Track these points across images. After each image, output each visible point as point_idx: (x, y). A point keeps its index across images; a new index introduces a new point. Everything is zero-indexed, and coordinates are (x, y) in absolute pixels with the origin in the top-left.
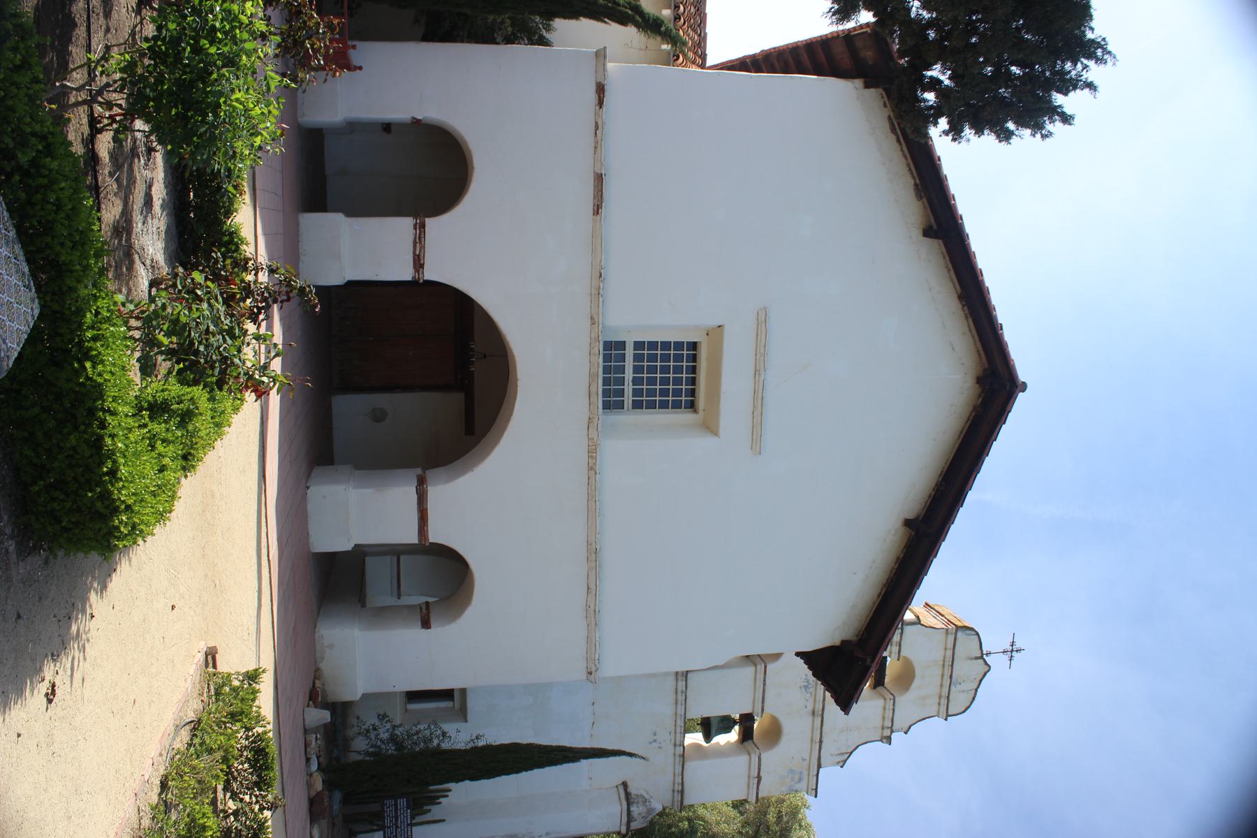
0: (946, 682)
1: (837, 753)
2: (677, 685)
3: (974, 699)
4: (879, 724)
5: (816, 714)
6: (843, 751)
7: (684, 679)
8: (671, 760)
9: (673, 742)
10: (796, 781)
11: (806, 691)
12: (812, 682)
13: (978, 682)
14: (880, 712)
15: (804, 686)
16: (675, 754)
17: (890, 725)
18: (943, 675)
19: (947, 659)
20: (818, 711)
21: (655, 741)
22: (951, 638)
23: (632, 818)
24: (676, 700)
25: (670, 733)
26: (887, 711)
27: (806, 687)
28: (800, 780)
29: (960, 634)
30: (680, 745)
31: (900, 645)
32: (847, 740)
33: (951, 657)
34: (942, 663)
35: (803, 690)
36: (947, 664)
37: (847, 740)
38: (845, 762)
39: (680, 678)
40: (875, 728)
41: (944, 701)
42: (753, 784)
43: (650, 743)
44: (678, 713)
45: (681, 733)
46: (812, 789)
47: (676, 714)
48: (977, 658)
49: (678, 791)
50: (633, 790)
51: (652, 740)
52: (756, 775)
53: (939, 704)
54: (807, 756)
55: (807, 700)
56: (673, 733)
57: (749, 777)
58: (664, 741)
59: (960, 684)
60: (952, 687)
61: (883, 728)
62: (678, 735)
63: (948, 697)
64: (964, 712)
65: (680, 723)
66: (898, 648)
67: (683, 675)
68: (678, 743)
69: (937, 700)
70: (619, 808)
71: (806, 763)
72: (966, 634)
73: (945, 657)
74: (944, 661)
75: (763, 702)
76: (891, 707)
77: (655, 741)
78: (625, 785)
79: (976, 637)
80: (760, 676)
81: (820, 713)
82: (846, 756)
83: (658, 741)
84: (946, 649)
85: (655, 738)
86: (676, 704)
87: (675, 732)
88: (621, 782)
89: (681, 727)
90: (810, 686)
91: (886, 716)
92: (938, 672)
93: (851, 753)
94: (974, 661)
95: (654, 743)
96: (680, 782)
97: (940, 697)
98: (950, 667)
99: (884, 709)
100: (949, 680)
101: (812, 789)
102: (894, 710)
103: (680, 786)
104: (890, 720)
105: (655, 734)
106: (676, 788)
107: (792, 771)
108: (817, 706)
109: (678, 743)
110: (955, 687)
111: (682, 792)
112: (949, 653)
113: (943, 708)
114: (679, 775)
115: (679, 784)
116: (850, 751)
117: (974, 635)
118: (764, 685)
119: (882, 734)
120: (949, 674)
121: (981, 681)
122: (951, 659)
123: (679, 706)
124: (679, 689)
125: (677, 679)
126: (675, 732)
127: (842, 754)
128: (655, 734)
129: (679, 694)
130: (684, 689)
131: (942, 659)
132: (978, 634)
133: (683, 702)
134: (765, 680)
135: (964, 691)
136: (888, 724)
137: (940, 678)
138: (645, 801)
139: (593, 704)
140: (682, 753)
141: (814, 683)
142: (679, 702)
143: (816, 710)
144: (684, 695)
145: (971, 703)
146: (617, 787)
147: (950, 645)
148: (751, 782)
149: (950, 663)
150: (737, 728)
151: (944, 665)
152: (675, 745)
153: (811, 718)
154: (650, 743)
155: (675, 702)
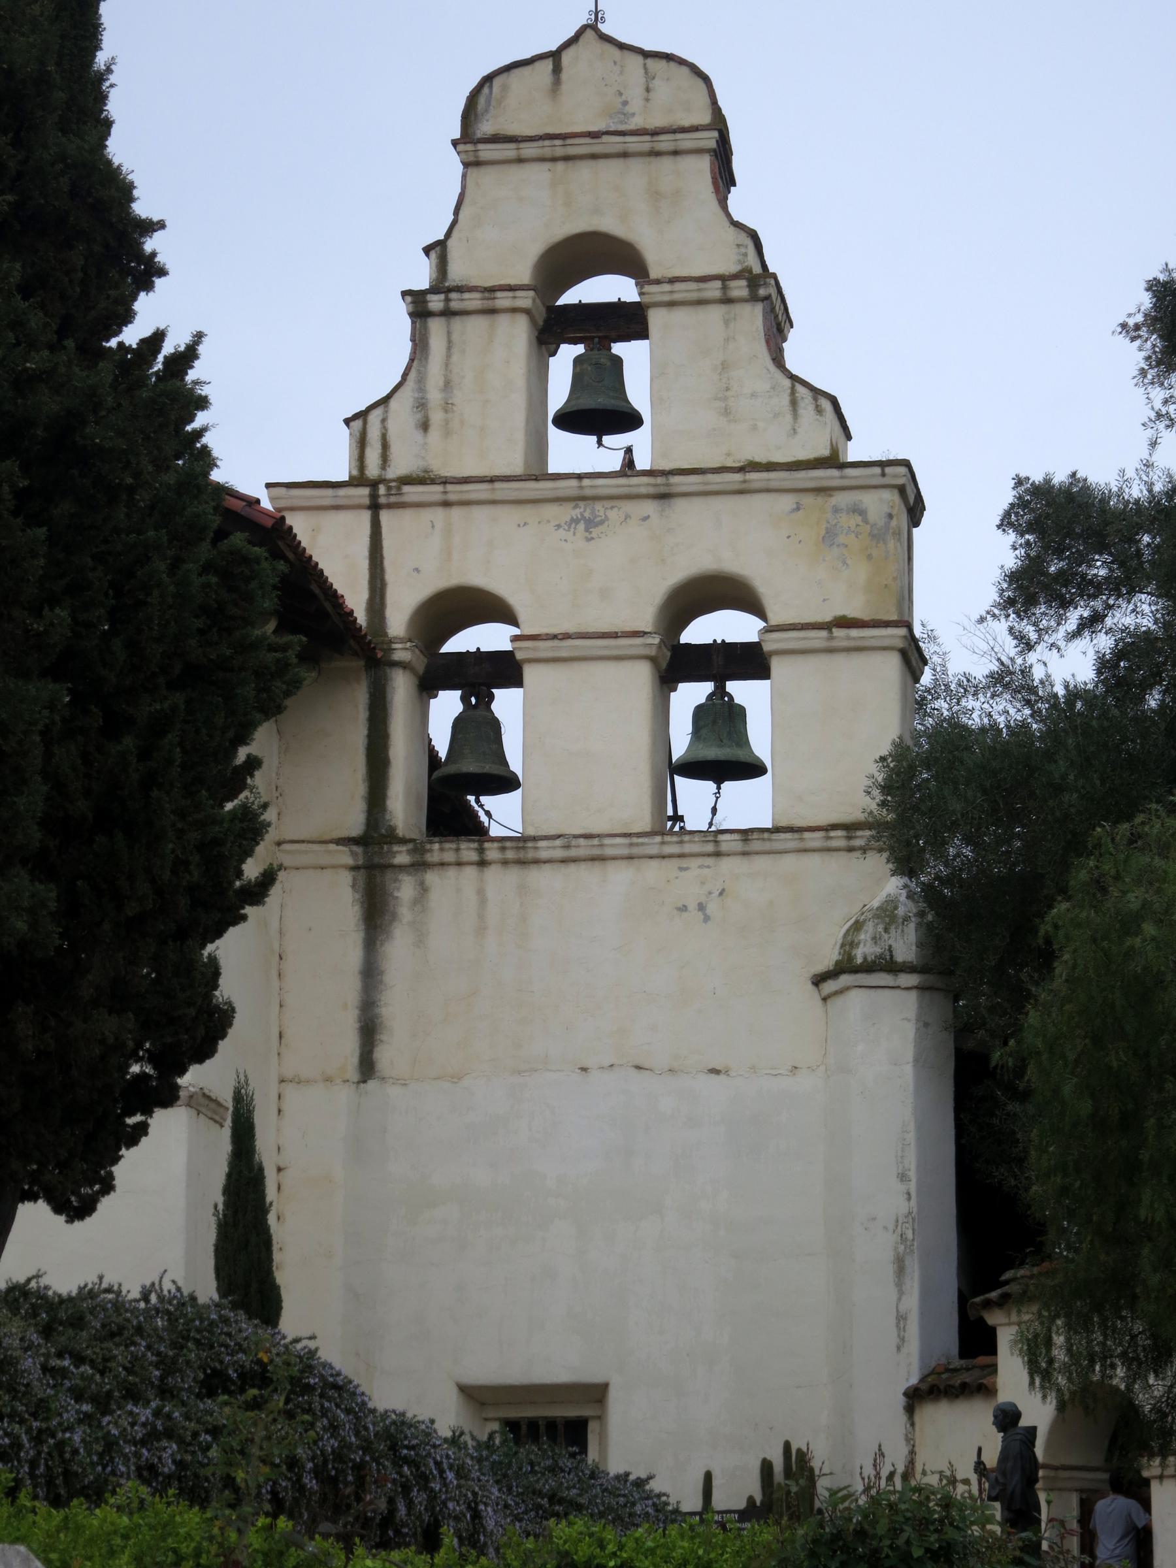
0: (612, 144)
1: (788, 417)
2: (614, 858)
3: (669, 57)
4: (715, 313)
5: (662, 490)
6: (785, 400)
7: (530, 844)
8: (761, 863)
9: (709, 861)
10: (859, 519)
11: (602, 522)
12: (578, 511)
13: (626, 53)
14: (680, 316)
15: (587, 530)
16: (745, 854)
17: (718, 284)
18: (594, 157)
19: (548, 152)
20: (656, 485)
21: (701, 907)
22: (487, 152)
23: (881, 956)
24: (593, 859)
25: (681, 869)
26: (677, 297)
27: (590, 524)
28: (858, 510)
29: (486, 128)
30: (716, 842)
31: (492, 290)
32: (753, 395)
33: (540, 143)
34: (560, 166)
35: (595, 532)
36: (560, 152)
37: (753, 395)
38: (816, 392)
39: (531, 855)
40: (727, 322)
41: (665, 142)
42: (848, 638)
43: (707, 919)
44: (625, 851)
45: (681, 842)
46: (883, 475)
47: (630, 858)
48: (557, 70)
49: (849, 838)
50: (828, 957)
51: (701, 916)
52: (824, 634)
53: (676, 153)
54: (786, 502)
55: (627, 517)
56: (685, 863)
57: (830, 651)
58: (703, 883)
59: (625, 103)
60: (635, 123)
61: (727, 301)
62: (688, 848)
63: (655, 133)
64: (706, 79)
65: (653, 845)
66: (499, 294)
67: (524, 848)
68: (710, 848)
69: (667, 163)
70: (854, 993)
71: (808, 500)
72: (487, 111)
73: (542, 159)
74: (554, 160)
75: (614, 635)
76: (667, 287)
77: (701, 907)
78: (819, 980)
79: (497, 82)
80: (544, 648)
81: (660, 480)
82: (801, 390)
83: (703, 899)
84: (520, 160)
85: (692, 906)
86: (602, 859)
87: (681, 856)
88: (814, 988)
89: (663, 843)
90: (587, 515)
91: (694, 296)
92: (584, 172)
93: (794, 378)
94: (564, 76)
95: (708, 911)
96: (821, 834)
97: (655, 154)
98: (569, 141)
99: (671, 304)
100: (605, 138)
101: (883, 475)
102: (673, 280)
103: (833, 834)
104: (702, 285)
105: (684, 909)
106: (842, 843)
107: (829, 537)
108: (643, 490)
109: (710, 848)
110: (633, 114)
111: (850, 828)
112: (529, 150)
113: (687, 141)
114: (801, 839)
115: (828, 838)
116: (787, 383)
117: (491, 87)
118: (567, 636)
119: (746, 301)
120: (588, 140)
121: (622, 46)
122: (547, 143)
123: (609, 852)
124: (559, 854)
125: (537, 862)
126: (681, 856)
127: (794, 403)
128: (684, 909)
129: (573, 853)
130: (558, 842)
131: (548, 165)
132: (488, 79)
133: (596, 842)
134: (554, 637)
135: (648, 90)
136: (713, 290)
137: (602, 163)
138: (857, 926)
139: (584, 1069)
140: (736, 836)
141: (582, 504)
142: (597, 852)
143: (651, 490)
144: (574, 842)
145: (682, 62)
146: (825, 999)
147: (507, 151)
148: (845, 644)
149: (558, 142)
150: (732, 687)
151: (567, 158)
152: (718, 854)
153: (680, 504)
154: (707, 919)
155: (597, 863)
